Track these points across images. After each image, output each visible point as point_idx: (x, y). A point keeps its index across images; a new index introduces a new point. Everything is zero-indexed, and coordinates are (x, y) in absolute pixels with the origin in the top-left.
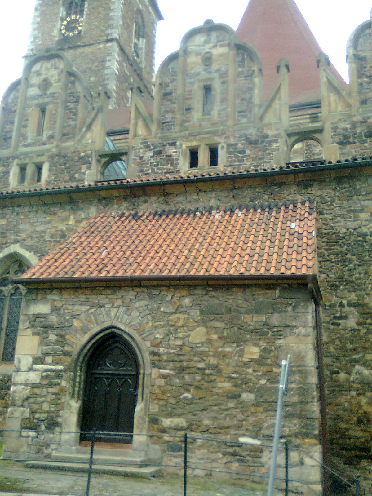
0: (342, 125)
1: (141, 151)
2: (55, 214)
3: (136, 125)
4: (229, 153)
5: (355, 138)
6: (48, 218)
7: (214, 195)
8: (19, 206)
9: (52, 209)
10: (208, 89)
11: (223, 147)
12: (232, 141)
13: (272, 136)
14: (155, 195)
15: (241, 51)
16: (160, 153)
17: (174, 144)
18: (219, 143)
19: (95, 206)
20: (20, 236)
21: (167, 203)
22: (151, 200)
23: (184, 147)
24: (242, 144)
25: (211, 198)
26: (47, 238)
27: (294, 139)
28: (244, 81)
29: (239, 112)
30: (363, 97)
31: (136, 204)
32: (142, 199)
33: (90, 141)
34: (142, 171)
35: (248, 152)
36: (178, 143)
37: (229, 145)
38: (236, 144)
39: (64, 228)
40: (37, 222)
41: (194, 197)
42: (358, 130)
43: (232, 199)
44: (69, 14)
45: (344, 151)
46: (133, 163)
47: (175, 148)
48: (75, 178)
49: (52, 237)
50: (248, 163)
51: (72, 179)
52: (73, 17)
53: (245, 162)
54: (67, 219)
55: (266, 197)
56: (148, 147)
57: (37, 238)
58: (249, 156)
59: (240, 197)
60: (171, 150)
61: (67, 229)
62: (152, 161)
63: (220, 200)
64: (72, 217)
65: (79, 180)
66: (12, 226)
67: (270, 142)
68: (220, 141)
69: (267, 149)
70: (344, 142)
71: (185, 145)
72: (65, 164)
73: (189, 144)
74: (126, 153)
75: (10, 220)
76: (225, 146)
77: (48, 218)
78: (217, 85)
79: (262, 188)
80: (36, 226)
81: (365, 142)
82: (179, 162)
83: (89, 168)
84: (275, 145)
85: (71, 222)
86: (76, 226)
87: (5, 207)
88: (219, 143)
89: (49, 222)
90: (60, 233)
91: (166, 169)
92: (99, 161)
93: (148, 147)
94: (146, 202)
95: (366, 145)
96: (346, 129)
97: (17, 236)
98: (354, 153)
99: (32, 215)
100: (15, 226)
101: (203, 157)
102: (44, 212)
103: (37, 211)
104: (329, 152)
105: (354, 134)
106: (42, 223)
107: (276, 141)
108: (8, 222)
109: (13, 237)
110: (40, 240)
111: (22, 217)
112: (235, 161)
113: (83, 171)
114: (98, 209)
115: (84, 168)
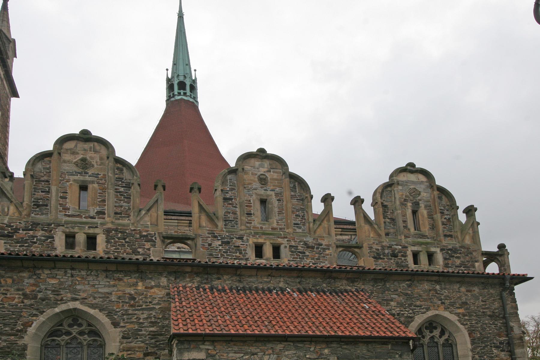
0: (375, 247)
1: (209, 239)
2: (120, 280)
3: (200, 217)
4: (292, 252)
5: (384, 256)
6: (112, 283)
7: (282, 279)
8: (73, 269)
9: (117, 275)
10: (263, 202)
11: (286, 247)
12: (293, 243)
13: (326, 245)
14: (227, 275)
15: (292, 180)
16: (228, 243)
17: (241, 238)
18: (282, 244)
19: (166, 277)
20: (80, 295)
21: (240, 281)
22: (225, 278)
23: (251, 242)
24: (302, 247)
25: (280, 281)
27: (341, 249)
28: (297, 203)
29: (294, 224)
30: (387, 231)
31: (209, 280)
32: (215, 276)
33: (149, 223)
34: (211, 255)
35: (307, 253)
36: (245, 238)
37: (290, 246)
38: (297, 247)
40: (99, 284)
41: (266, 280)
42: (386, 251)
43: (298, 284)
45: (377, 263)
46: (202, 247)
47: (243, 242)
48: (139, 252)
49: (119, 298)
50: (308, 261)
51: (135, 252)
53: (305, 260)
54: (135, 285)
55: (325, 285)
56: (216, 237)
57: (100, 298)
58: (308, 256)
59: (304, 283)
60: (239, 243)
61: (136, 293)
62: (220, 248)
63: (288, 284)
64: (140, 284)
65: (142, 254)
66: (66, 286)
67: (324, 249)
68: (284, 242)
69: (321, 254)
70: (377, 257)
71: (252, 241)
72: (125, 239)
73: (255, 240)
74: (193, 239)
75: (62, 280)
76: (288, 246)
77: (112, 283)
78: (274, 200)
79: (321, 279)
81: (391, 259)
82: (247, 252)
83: (154, 246)
84: (327, 252)
85: (139, 288)
86: (145, 291)
87: (54, 269)
88: (282, 244)
91: (236, 256)
92: (163, 242)
93: (216, 237)
94: (219, 279)
95: (392, 261)
96: (378, 250)
97: (75, 294)
98: (384, 265)
99: (91, 278)
100: (70, 286)
101: (268, 251)
102: (107, 277)
103: (97, 276)
104: (367, 262)
105: (384, 254)
106: (105, 286)
107: (329, 249)
109: (69, 295)
110: (106, 300)
111: (79, 279)
112: (297, 258)
113: (146, 247)
114: (169, 280)
115: (148, 245)
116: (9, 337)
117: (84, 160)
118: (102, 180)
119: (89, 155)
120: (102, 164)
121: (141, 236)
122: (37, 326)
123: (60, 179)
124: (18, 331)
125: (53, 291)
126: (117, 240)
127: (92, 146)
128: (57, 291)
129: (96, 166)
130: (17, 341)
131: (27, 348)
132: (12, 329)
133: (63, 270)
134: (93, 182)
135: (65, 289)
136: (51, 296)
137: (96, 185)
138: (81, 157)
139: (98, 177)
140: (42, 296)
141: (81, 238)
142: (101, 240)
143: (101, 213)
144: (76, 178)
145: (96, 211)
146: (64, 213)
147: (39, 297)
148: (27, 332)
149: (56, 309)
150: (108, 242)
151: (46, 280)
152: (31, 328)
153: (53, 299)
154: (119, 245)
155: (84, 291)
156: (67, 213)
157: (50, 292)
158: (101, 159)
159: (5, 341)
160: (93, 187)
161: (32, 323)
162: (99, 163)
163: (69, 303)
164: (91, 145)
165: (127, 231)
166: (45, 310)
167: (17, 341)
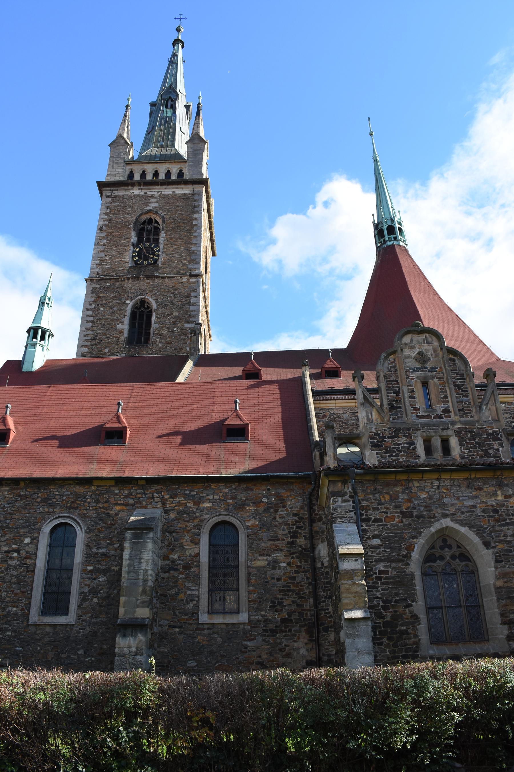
26: (478, 511)
39: (494, 503)
44: (140, 241)
52: (147, 245)
80: (463, 500)
89: (476, 497)
90: (491, 508)
97: (445, 510)
100: (438, 500)
108: (429, 495)
116: (397, 564)
117: (421, 353)
118: (439, 373)
119: (425, 347)
120: (437, 356)
121: (489, 435)
122: (419, 550)
123: (406, 376)
124: (404, 556)
125: (425, 507)
126: (468, 441)
127: (424, 337)
128: (429, 507)
129: (432, 359)
130: (404, 568)
131: (414, 576)
132: (398, 555)
133: (430, 481)
134: (433, 378)
135: (434, 503)
136: (425, 513)
137: (436, 380)
138: (417, 350)
139: (436, 371)
140: (417, 513)
141: (437, 443)
142: (454, 442)
143: (446, 411)
144: (418, 374)
145: (442, 409)
146: (416, 415)
147: (414, 515)
148: (412, 558)
149: (431, 528)
150: (461, 444)
151: (417, 494)
152: (414, 553)
153: (426, 516)
154: (471, 447)
155: (452, 505)
156: (418, 415)
157: (423, 508)
158: (435, 351)
159: (395, 568)
160: (434, 382)
161: (414, 546)
162: (434, 356)
163: (441, 521)
164: (423, 336)
165: (475, 430)
166: (422, 530)
167: (404, 568)
